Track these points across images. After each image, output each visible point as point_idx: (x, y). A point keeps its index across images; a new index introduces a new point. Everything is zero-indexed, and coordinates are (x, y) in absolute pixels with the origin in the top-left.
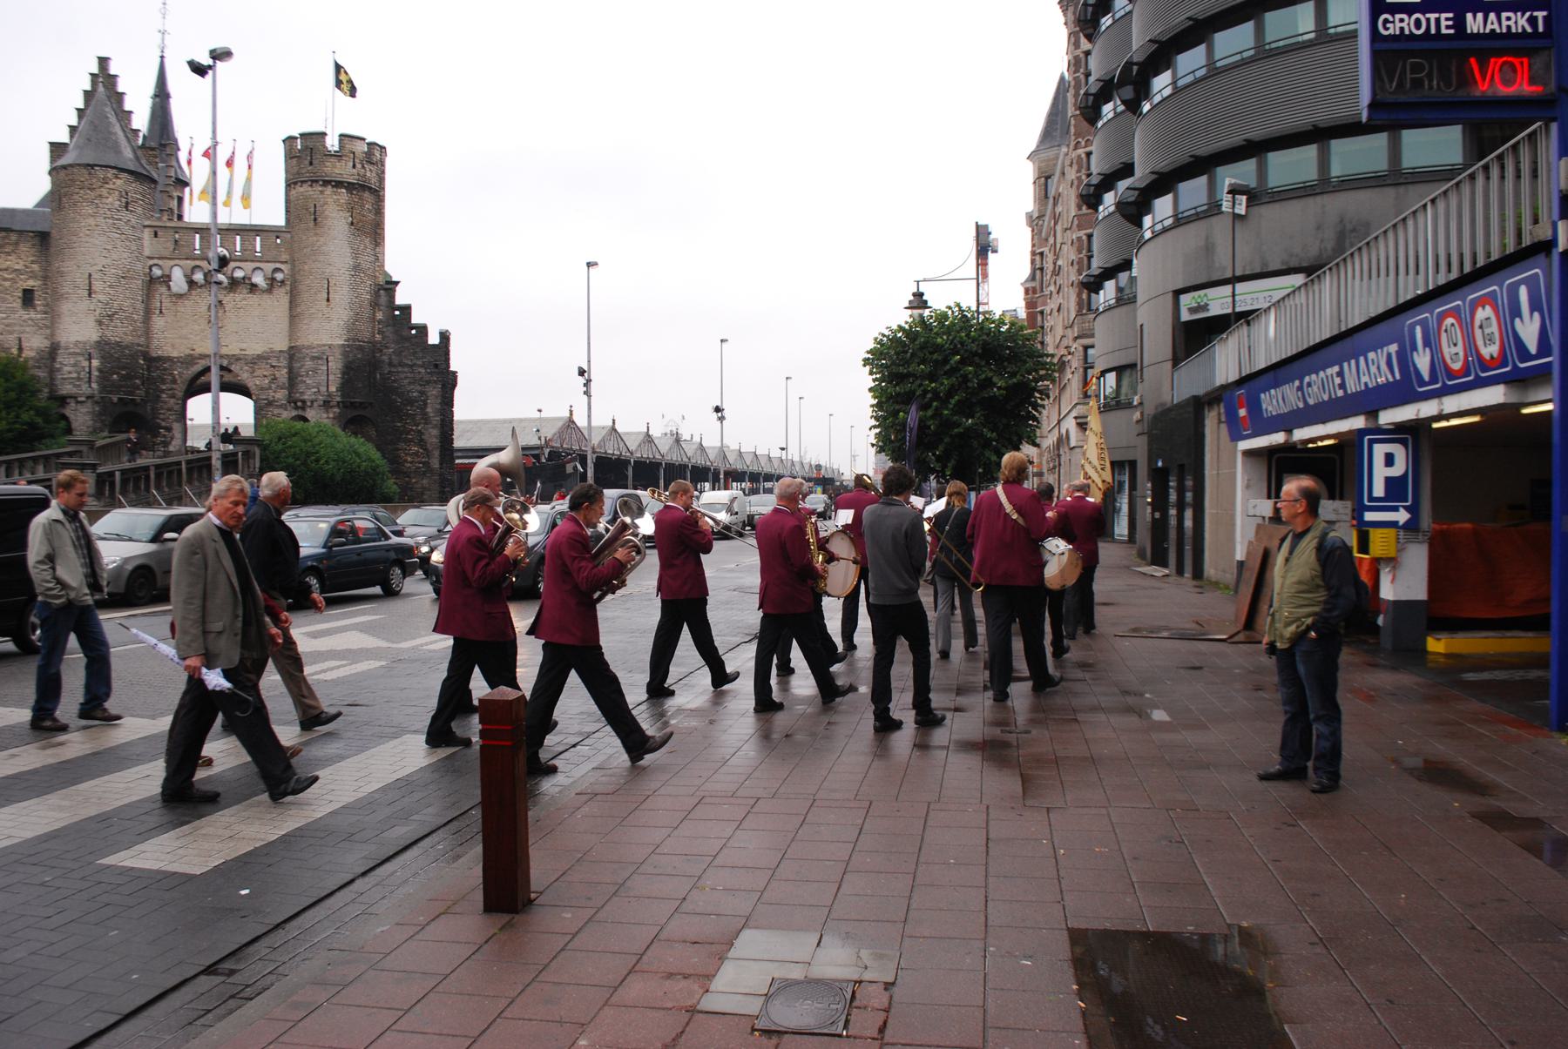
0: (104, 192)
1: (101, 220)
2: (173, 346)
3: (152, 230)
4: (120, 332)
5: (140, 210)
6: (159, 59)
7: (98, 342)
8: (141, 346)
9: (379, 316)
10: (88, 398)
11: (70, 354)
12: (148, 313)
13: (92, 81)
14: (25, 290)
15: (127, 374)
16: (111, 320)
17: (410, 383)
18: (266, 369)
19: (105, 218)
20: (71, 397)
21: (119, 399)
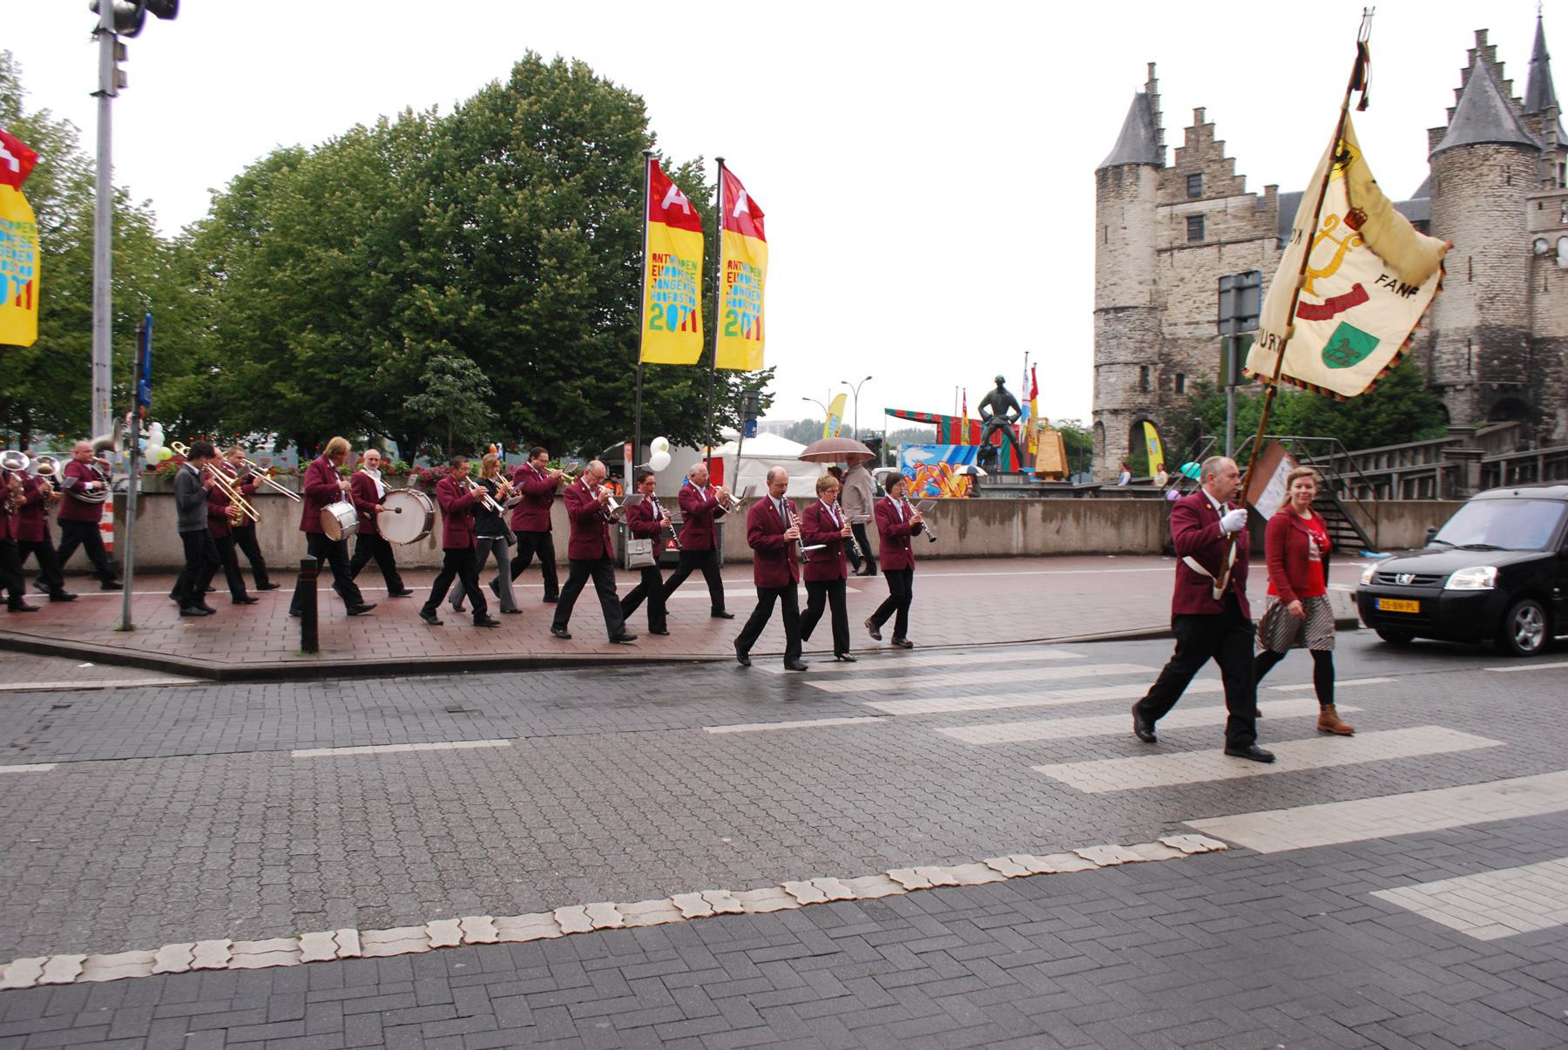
0: (1485, 170)
1: (1482, 200)
2: (1559, 325)
4: (1502, 316)
5: (1522, 183)
6: (1535, 21)
7: (1478, 327)
10: (1467, 385)
11: (1449, 341)
12: (1532, 291)
19: (1486, 197)
20: (1449, 386)
21: (1501, 385)
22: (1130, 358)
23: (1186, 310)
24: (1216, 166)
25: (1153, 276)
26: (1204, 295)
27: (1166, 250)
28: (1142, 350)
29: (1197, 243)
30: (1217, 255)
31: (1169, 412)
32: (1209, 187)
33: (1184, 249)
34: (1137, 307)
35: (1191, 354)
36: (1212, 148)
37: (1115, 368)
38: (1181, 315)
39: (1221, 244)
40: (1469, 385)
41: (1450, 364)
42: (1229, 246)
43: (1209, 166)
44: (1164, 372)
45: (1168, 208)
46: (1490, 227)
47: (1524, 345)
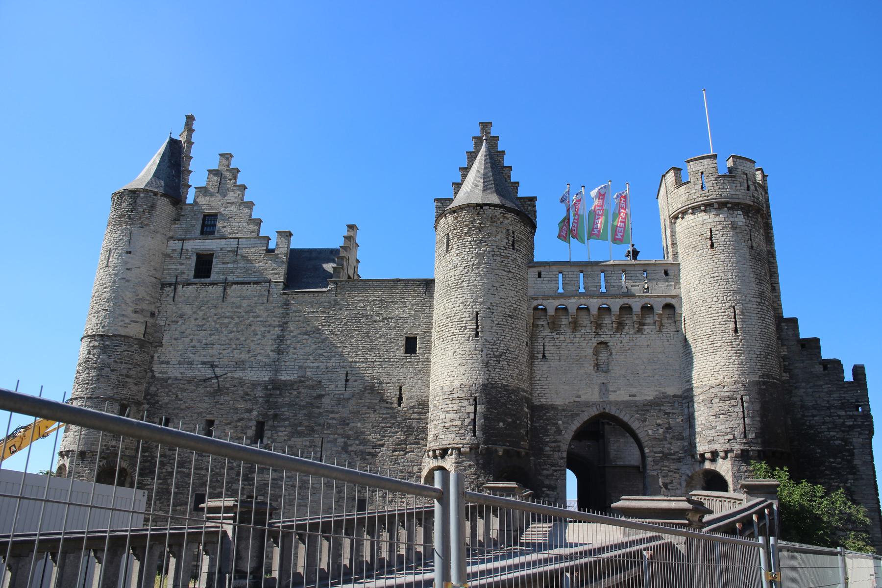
3: (536, 270)
7: (483, 385)
8: (526, 392)
9: (784, 352)
13: (475, 144)
14: (408, 339)
15: (514, 422)
17: (829, 430)
18: (659, 418)
19: (493, 255)
25: (152, 308)
26: (202, 333)
27: (170, 285)
30: (222, 295)
33: (189, 284)
35: (180, 397)
39: (226, 284)
41: (454, 423)
42: (234, 286)
46: (497, 285)
47: (527, 410)
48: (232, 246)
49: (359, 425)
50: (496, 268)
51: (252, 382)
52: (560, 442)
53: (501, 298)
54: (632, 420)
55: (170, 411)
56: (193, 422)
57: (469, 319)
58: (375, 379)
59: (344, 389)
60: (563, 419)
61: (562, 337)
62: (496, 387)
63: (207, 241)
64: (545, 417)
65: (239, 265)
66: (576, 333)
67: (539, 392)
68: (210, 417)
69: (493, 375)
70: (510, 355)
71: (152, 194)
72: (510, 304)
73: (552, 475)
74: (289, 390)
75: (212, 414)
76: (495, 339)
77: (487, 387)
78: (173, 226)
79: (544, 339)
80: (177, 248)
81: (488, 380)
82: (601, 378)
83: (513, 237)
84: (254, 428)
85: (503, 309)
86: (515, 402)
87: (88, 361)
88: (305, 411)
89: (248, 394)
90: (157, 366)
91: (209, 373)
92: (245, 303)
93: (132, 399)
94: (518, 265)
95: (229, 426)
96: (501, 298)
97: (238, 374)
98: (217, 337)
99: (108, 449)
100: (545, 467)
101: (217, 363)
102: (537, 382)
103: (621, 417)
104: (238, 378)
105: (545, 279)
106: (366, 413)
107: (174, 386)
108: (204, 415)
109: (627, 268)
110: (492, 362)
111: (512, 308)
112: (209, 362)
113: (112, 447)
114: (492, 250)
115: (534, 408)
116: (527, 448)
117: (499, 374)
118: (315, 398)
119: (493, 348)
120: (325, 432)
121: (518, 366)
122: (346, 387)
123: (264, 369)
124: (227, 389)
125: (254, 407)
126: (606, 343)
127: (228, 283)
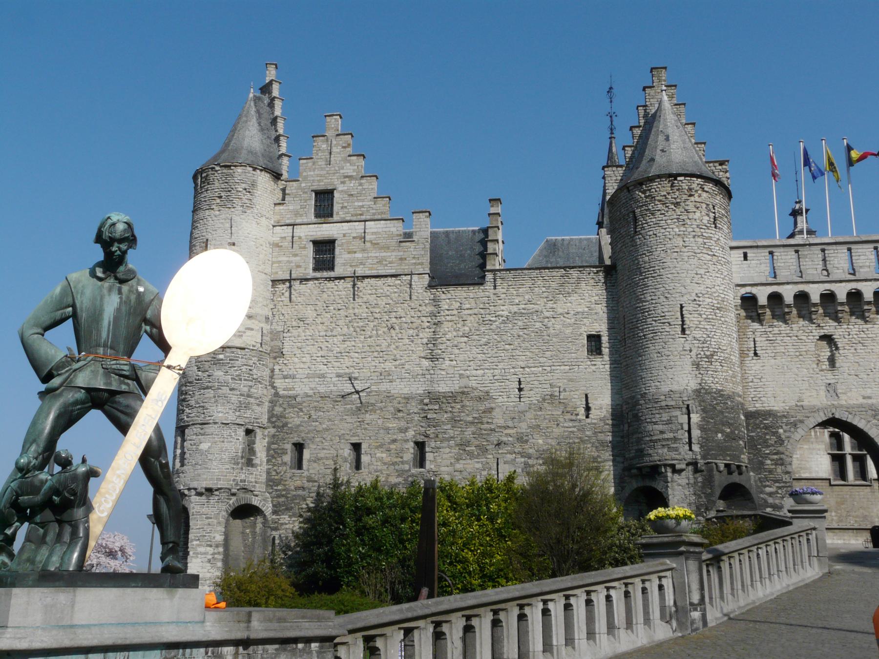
1: (689, 240)
3: (741, 251)
7: (697, 392)
11: (661, 408)
14: (590, 337)
15: (732, 432)
16: (712, 362)
19: (694, 237)
20: (665, 465)
22: (231, 417)
23: (307, 359)
24: (352, 184)
25: (267, 312)
27: (283, 281)
28: (247, 406)
29: (326, 274)
31: (278, 496)
32: (342, 208)
33: (307, 280)
34: (244, 349)
35: (314, 417)
36: (349, 161)
37: (209, 429)
38: (302, 366)
40: (694, 464)
41: (665, 436)
43: (343, 183)
44: (274, 440)
45: (291, 227)
46: (702, 271)
47: (743, 417)
48: (358, 231)
49: (541, 441)
50: (699, 251)
51: (403, 396)
52: (783, 453)
53: (707, 287)
54: (869, 426)
55: (303, 435)
56: (334, 447)
57: (673, 313)
58: (555, 386)
59: (518, 400)
60: (784, 427)
61: (776, 330)
62: (709, 393)
63: (324, 225)
64: (762, 426)
65: (370, 255)
66: (793, 326)
67: (752, 396)
68: (355, 440)
69: (707, 379)
70: (722, 355)
71: (251, 169)
72: (717, 294)
73: (777, 492)
74: (449, 403)
75: (358, 436)
76: (705, 336)
77: (700, 392)
78: (276, 208)
79: (754, 333)
80: (286, 235)
81: (700, 384)
82: (830, 377)
83: (714, 213)
84: (412, 451)
85: (710, 300)
86: (732, 409)
87: (198, 380)
88: (472, 429)
89: (399, 411)
90: (279, 381)
91: (349, 388)
92: (382, 302)
93: (257, 423)
94: (722, 246)
95: (382, 449)
96: (707, 287)
97: (384, 386)
98: (353, 343)
99: (237, 484)
100: (768, 483)
101: (357, 375)
102: (750, 384)
103: (855, 423)
104: (385, 391)
105: (752, 262)
106: (547, 428)
107: (304, 404)
108: (347, 437)
109: (853, 246)
110: (703, 363)
111: (720, 298)
112: (346, 374)
113: (241, 481)
114: (692, 230)
115: (749, 415)
116: (747, 462)
117: (713, 377)
118: (484, 412)
119: (703, 347)
120: (500, 452)
121: (731, 368)
122: (520, 398)
123: (416, 380)
124: (373, 405)
125: (409, 425)
126: (832, 335)
127: (357, 277)
